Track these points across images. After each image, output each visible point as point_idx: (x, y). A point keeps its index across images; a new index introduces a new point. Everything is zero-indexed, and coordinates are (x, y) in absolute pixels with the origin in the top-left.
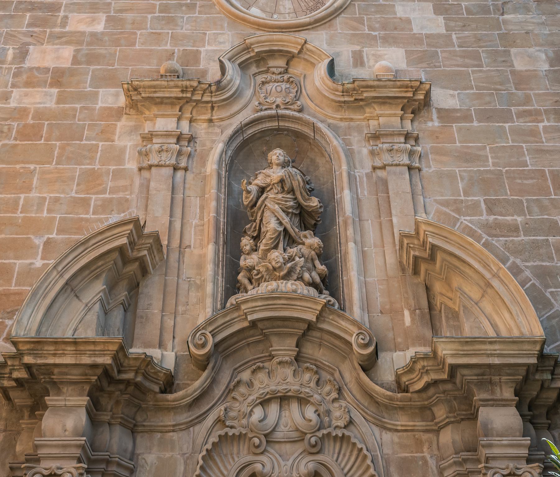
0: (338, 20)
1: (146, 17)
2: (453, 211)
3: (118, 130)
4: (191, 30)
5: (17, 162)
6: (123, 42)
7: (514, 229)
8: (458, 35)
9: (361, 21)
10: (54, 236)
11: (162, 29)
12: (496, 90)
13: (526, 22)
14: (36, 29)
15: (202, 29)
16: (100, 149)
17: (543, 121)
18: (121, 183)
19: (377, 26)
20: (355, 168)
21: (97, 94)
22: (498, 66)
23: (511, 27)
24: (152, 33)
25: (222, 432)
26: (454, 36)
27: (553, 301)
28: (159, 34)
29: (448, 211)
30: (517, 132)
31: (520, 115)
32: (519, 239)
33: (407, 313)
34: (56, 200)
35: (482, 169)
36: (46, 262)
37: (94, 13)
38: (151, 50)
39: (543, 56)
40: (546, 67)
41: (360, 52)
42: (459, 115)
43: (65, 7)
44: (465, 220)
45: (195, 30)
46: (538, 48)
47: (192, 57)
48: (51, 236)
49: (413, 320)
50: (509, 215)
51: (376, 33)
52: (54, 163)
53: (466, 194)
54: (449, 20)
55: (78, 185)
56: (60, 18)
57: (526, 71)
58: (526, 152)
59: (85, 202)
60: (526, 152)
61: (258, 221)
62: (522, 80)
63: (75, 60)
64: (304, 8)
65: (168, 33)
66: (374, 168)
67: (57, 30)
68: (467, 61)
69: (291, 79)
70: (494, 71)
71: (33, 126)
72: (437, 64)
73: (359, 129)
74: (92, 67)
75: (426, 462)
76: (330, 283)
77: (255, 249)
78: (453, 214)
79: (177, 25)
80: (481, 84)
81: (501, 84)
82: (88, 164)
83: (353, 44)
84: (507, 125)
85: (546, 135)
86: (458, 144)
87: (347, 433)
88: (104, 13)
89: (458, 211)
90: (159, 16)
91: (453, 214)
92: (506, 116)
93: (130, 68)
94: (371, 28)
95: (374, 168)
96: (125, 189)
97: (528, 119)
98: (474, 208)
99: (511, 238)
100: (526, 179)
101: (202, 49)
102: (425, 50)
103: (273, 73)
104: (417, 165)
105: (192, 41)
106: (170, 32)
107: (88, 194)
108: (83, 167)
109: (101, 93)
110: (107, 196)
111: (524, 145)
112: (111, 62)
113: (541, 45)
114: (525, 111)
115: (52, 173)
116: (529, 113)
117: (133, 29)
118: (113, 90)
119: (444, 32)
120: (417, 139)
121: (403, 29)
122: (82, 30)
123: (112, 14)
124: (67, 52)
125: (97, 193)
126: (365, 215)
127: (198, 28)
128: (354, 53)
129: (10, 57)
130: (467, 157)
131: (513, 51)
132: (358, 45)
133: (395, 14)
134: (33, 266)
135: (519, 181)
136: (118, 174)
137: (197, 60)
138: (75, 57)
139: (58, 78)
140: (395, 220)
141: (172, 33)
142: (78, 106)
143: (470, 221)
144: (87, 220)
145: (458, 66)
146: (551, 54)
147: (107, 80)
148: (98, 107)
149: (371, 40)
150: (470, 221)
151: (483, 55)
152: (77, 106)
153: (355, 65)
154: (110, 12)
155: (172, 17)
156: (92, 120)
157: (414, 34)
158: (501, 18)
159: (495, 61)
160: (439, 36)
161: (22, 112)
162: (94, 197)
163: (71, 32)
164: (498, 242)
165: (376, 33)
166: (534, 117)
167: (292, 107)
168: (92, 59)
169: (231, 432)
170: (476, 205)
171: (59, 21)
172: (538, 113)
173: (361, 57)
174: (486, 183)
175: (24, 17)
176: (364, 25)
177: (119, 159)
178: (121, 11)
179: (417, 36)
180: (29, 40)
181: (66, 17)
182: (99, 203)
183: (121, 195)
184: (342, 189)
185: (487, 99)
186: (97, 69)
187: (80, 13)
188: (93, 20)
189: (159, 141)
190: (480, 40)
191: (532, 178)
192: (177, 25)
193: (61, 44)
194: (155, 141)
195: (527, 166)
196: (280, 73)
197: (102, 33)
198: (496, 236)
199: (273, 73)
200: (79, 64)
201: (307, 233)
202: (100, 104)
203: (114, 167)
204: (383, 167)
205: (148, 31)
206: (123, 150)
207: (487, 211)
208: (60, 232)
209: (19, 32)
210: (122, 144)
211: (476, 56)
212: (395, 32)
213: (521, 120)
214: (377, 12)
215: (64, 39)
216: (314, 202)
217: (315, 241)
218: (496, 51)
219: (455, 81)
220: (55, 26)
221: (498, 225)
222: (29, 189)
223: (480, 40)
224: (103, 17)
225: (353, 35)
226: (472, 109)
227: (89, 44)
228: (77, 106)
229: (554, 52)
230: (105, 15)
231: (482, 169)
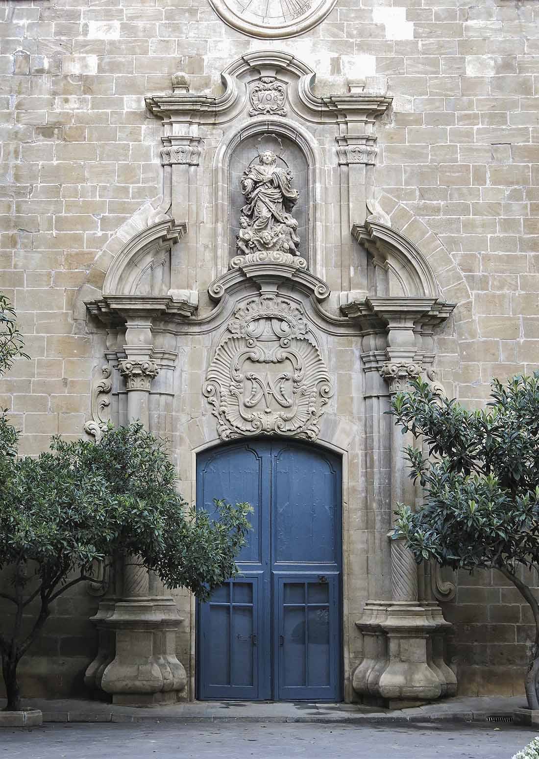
0: (322, 26)
1: (155, 24)
2: (394, 197)
3: (143, 132)
4: (194, 37)
5: (70, 159)
6: (138, 50)
7: (437, 210)
8: (424, 43)
10: (107, 214)
11: (169, 36)
12: (446, 95)
13: (486, 28)
14: (63, 38)
15: (204, 36)
16: (131, 147)
17: (478, 124)
18: (150, 175)
19: (355, 32)
20: (325, 164)
21: (122, 99)
22: (452, 73)
23: (470, 34)
24: (162, 40)
25: (230, 336)
26: (420, 43)
27: (453, 260)
28: (168, 42)
29: (391, 196)
30: (456, 134)
31: (462, 118)
32: (439, 217)
33: (352, 269)
34: (104, 188)
35: (422, 164)
36: (104, 232)
37: (109, 20)
38: (162, 58)
39: (492, 63)
40: (492, 74)
41: (338, 59)
42: (411, 118)
43: (84, 14)
44: (403, 204)
45: (198, 38)
46: (489, 55)
47: (196, 64)
48: (105, 215)
49: (355, 273)
50: (435, 200)
51: (351, 40)
52: (98, 159)
53: (407, 184)
54: (418, 26)
55: (118, 176)
56: (81, 26)
57: (475, 77)
58: (459, 151)
59: (126, 190)
60: (459, 151)
61: (253, 204)
62: (470, 86)
63: (100, 69)
64: (292, 11)
65: (175, 40)
66: (340, 165)
67: (81, 38)
68: (428, 68)
69: (280, 88)
70: (448, 77)
71: (76, 128)
72: (401, 71)
73: (331, 133)
74: (116, 75)
75: (353, 352)
78: (394, 199)
79: (181, 33)
80: (435, 91)
81: (451, 90)
82: (124, 160)
83: (333, 51)
84: (448, 128)
85: (477, 136)
86: (407, 144)
87: (307, 337)
88: (118, 20)
89: (398, 197)
90: (166, 23)
91: (394, 199)
92: (448, 119)
93: (146, 75)
94: (350, 35)
95: (340, 165)
96: (153, 179)
97: (466, 122)
99: (433, 217)
100: (454, 172)
101: (204, 57)
102: (392, 59)
103: (265, 82)
104: (373, 163)
105: (196, 49)
106: (177, 39)
107: (126, 183)
108: (120, 162)
109: (125, 99)
110: (140, 185)
111: (458, 145)
112: (130, 70)
113: (493, 52)
114: (466, 115)
115: (97, 167)
116: (468, 116)
117: (144, 36)
118: (134, 97)
119: (412, 38)
120: (375, 140)
121: (376, 36)
122: (102, 39)
123: (125, 22)
124: (93, 61)
125: (132, 183)
126: (330, 200)
127: (200, 36)
128: (332, 59)
130: (412, 155)
131: (469, 58)
132: (337, 52)
133: (372, 20)
134: (96, 235)
135: (448, 174)
136: (147, 168)
137: (201, 68)
138: (99, 66)
140: (351, 205)
141: (178, 40)
142: (109, 111)
143: (406, 205)
144: (129, 203)
145: (419, 73)
146: (500, 61)
147: (131, 87)
148: (125, 112)
149: (347, 47)
150: (406, 205)
151: (442, 62)
152: (107, 111)
153: (333, 73)
154: (122, 20)
155: (178, 24)
156: (121, 123)
157: (386, 41)
158: (465, 24)
159: (450, 68)
160: (407, 43)
162: (131, 185)
163: (93, 41)
165: (351, 40)
166: (472, 121)
167: (279, 112)
168: (114, 67)
169: (235, 336)
170: (412, 192)
171: (81, 29)
172: (476, 116)
173: (339, 65)
174: (422, 175)
175: (49, 25)
176: (343, 31)
177: (147, 156)
178: (131, 18)
179: (389, 42)
180: (59, 49)
181: (86, 25)
182: (136, 190)
183: (151, 184)
184: (314, 182)
185: (437, 104)
186: (119, 77)
187: (97, 21)
188: (110, 28)
189: (177, 143)
190: (442, 47)
191: (459, 172)
192: (181, 33)
193: (87, 52)
194: (173, 143)
195: (457, 162)
196: (271, 82)
197: (119, 41)
198: (422, 215)
199: (265, 82)
200: (104, 72)
201: (287, 215)
202: (126, 110)
203: (143, 163)
204: (347, 164)
205: (158, 39)
206: (148, 148)
207: (420, 197)
208: (111, 211)
209: (49, 41)
210: (146, 143)
211: (435, 63)
212: (368, 40)
213: (461, 123)
214: (356, 18)
215: (88, 48)
218: (454, 59)
219: (414, 86)
220: (78, 34)
221: (425, 207)
222: (84, 180)
223: (442, 47)
224: (117, 24)
225: (334, 42)
226: (424, 113)
227: (110, 52)
228: (107, 111)
229: (502, 59)
230: (119, 22)
231: (422, 164)
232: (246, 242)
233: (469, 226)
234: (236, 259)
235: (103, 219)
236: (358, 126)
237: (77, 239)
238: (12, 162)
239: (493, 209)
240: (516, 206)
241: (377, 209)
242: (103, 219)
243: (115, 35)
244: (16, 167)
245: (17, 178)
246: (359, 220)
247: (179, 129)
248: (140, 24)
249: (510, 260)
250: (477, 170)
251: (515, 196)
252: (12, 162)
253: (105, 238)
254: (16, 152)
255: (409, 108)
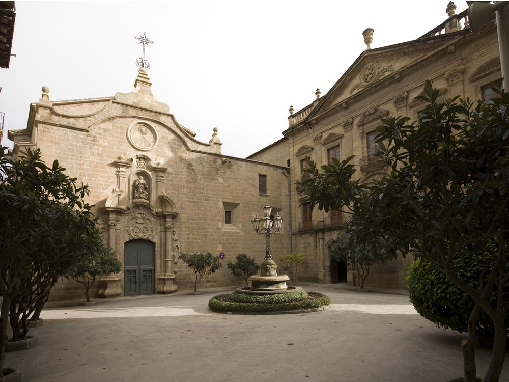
7: (176, 193)
9: (157, 151)
30: (180, 178)
44: (169, 191)
63: (102, 152)
76: (148, 199)
77: (137, 193)
98: (170, 190)
129: (88, 148)
130: (171, 181)
139: (99, 155)
147: (110, 157)
149: (158, 156)
161: (93, 162)
164: (173, 195)
178: (110, 140)
216: (147, 187)
217: (147, 193)
219: (172, 167)
232: (136, 197)
233: (181, 197)
234: (134, 200)
235: (103, 188)
236: (160, 174)
237: (96, 192)
238: (79, 171)
239: (186, 194)
240: (190, 194)
241: (164, 192)
242: (103, 188)
243: (106, 144)
244: (80, 172)
245: (80, 175)
246: (160, 194)
247: (122, 169)
248: (112, 142)
249: (189, 205)
250: (184, 186)
251: (190, 192)
252: (79, 171)
253: (103, 192)
254: (80, 168)
255: (171, 171)
